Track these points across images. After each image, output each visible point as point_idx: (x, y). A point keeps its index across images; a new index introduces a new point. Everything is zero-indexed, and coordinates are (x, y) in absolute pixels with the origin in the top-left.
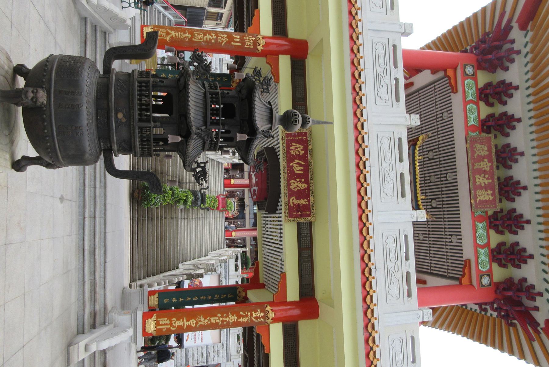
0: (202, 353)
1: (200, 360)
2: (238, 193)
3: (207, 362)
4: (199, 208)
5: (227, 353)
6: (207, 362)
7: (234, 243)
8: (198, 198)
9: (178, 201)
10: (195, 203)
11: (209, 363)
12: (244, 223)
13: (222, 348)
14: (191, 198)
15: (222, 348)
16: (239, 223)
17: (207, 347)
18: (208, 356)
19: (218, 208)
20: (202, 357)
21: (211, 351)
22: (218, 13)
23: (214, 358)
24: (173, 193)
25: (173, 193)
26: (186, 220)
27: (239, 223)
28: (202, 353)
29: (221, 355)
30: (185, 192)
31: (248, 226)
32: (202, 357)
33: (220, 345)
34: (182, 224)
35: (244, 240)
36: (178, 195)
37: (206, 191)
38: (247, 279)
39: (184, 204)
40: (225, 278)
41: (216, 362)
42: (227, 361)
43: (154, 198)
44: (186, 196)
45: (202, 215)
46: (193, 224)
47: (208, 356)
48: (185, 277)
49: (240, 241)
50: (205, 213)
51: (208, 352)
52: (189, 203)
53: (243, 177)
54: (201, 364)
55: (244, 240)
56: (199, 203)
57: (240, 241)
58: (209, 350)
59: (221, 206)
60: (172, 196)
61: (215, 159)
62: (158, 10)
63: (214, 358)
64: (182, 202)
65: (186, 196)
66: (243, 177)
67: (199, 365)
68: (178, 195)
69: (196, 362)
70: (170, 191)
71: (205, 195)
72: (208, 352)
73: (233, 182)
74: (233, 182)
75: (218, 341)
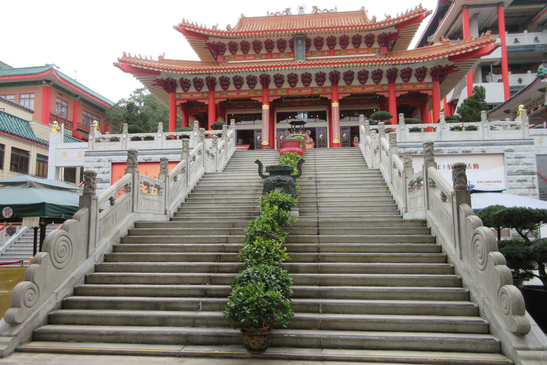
0: (519, 181)
1: (529, 184)
2: (281, 137)
3: (532, 173)
4: (297, 179)
5: (520, 144)
6: (532, 173)
7: (347, 142)
8: (279, 181)
9: (281, 221)
10: (288, 188)
11: (535, 170)
12: (320, 128)
13: (512, 151)
14: (277, 193)
15: (512, 151)
16: (321, 136)
17: (510, 174)
18: (524, 173)
19: (300, 153)
20: (525, 181)
21: (515, 168)
22: (37, 160)
23: (527, 164)
24: (262, 233)
25: (262, 233)
26: (319, 204)
27: (321, 136)
28: (519, 181)
29: (523, 154)
30: (263, 206)
31: (324, 124)
32: (525, 181)
33: (507, 154)
34: (327, 214)
35: (343, 129)
36: (268, 222)
37: (265, 164)
38: (405, 117)
39: (289, 209)
40: (404, 147)
41: (533, 161)
42: (532, 143)
43: (266, 289)
44: (272, 203)
45: (310, 178)
46: (326, 193)
47: (524, 173)
48: (464, 207)
49: (344, 135)
50: (307, 174)
51: (518, 173)
52: (288, 197)
53: (260, 131)
54: (536, 183)
55: (343, 129)
56: (288, 178)
57: (344, 135)
58: (515, 170)
59: (297, 149)
60: (268, 237)
61: (227, 162)
62: (15, 243)
63: (527, 164)
64: (283, 213)
65: (272, 203)
66: (260, 131)
67: (537, 186)
68: (268, 222)
69: (531, 190)
70: (256, 243)
71: (272, 167)
72: (518, 173)
73: (265, 143)
74: (265, 143)
75: (500, 158)
